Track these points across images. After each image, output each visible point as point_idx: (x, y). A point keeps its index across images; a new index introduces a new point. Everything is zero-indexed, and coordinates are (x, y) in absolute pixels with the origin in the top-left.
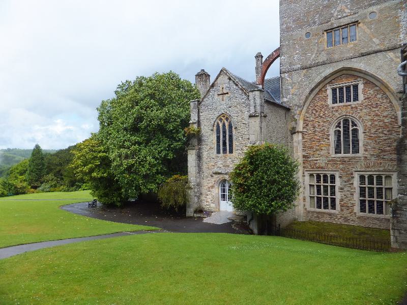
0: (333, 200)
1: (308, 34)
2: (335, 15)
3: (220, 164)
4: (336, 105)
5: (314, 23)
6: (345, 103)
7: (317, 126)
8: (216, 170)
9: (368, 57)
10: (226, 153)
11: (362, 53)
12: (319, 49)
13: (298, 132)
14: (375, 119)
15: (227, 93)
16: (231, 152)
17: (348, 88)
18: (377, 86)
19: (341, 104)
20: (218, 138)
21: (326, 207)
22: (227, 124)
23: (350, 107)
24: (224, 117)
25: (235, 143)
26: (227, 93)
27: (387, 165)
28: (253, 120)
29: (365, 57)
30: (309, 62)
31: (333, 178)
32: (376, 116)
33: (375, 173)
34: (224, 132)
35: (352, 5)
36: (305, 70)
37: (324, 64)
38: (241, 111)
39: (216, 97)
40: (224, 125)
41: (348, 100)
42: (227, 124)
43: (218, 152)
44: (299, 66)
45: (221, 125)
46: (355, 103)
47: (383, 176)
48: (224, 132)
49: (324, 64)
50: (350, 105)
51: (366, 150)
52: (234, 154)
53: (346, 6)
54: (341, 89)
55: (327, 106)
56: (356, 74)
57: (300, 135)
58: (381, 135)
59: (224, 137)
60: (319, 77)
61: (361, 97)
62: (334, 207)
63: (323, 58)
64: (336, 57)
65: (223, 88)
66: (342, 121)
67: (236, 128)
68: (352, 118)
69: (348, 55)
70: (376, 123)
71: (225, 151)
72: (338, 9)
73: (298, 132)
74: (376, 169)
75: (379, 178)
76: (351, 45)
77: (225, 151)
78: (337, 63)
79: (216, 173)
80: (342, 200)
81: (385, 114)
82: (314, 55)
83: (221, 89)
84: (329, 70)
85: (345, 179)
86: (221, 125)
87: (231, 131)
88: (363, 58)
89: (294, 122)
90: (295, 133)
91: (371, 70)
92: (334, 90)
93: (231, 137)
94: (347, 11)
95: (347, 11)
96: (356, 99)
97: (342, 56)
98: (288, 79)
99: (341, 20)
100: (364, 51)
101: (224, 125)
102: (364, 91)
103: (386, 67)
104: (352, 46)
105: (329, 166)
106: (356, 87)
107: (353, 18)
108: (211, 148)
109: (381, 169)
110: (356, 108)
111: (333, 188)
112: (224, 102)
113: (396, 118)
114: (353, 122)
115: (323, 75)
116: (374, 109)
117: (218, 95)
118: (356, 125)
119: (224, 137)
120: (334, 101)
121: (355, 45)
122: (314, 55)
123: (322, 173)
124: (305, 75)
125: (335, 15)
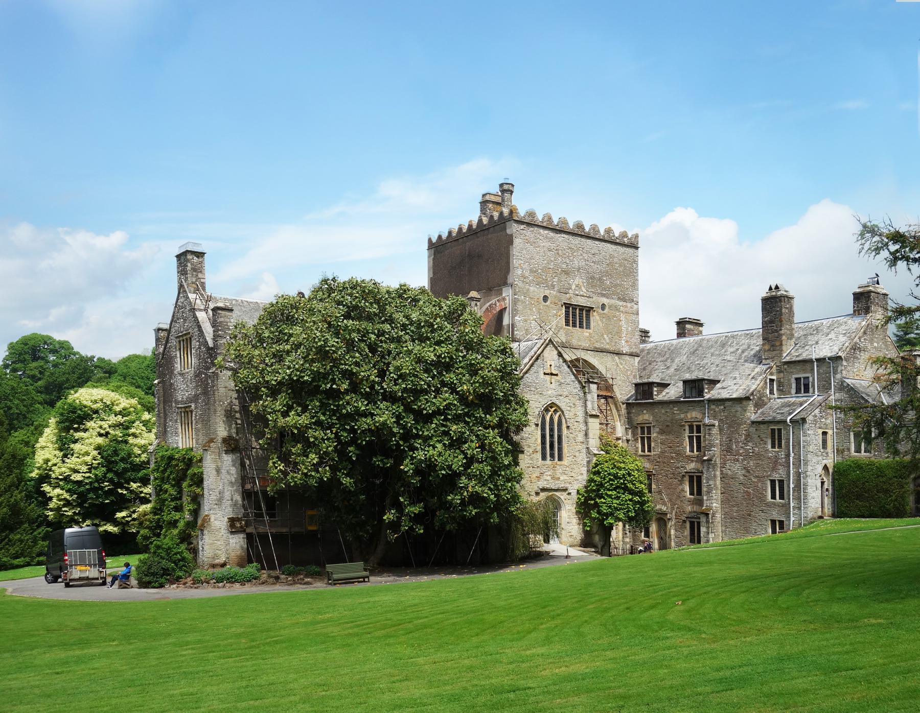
1: (545, 298)
5: (553, 286)
8: (542, 484)
15: (557, 375)
16: (560, 459)
20: (543, 437)
24: (552, 407)
25: (565, 445)
28: (591, 420)
34: (552, 430)
35: (588, 283)
40: (552, 419)
43: (544, 458)
45: (548, 418)
48: (552, 430)
52: (565, 462)
59: (552, 436)
64: (575, 342)
67: (568, 427)
71: (552, 456)
76: (586, 333)
77: (552, 456)
79: (543, 490)
86: (548, 418)
87: (560, 430)
91: (601, 369)
93: (560, 437)
100: (598, 345)
101: (552, 419)
108: (535, 451)
112: (553, 386)
119: (552, 436)
121: (591, 336)
125: (573, 287)
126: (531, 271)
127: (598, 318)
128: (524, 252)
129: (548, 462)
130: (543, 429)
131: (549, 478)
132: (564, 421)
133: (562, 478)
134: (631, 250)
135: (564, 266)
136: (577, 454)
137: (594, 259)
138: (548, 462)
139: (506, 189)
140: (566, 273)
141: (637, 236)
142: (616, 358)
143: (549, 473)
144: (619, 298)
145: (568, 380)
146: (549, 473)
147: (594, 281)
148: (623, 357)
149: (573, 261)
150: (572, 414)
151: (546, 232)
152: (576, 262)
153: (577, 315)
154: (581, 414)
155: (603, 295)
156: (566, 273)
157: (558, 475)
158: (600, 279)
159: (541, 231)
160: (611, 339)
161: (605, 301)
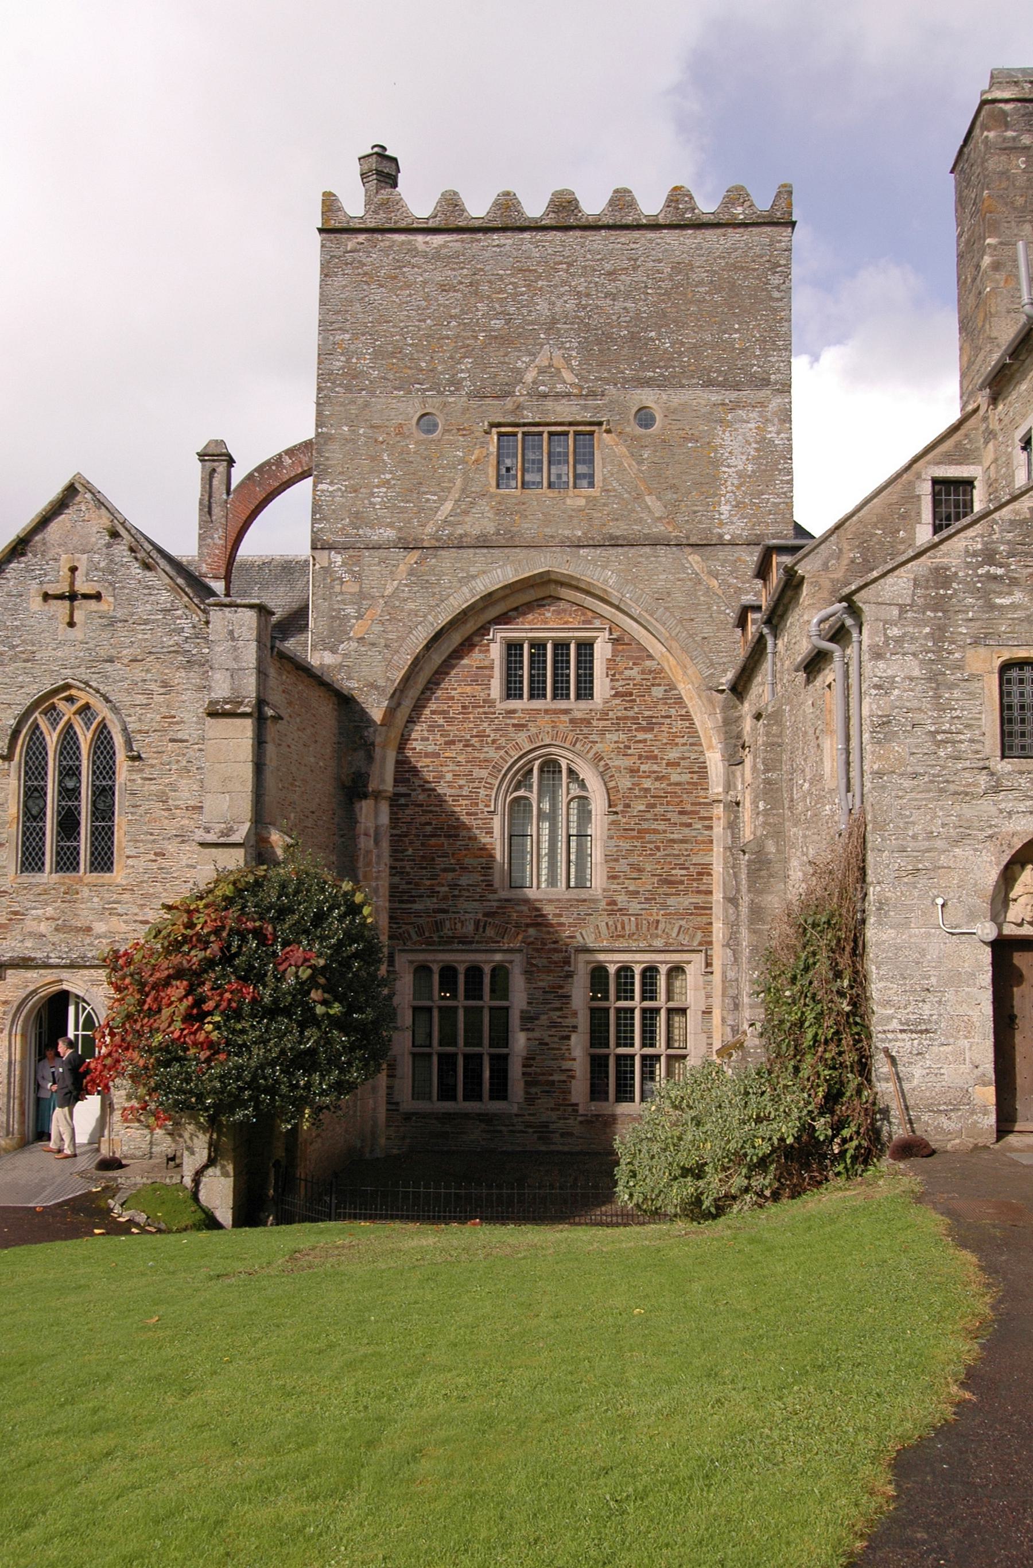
0: (500, 1064)
2: (529, 377)
3: (40, 920)
4: (514, 704)
6: (547, 703)
7: (449, 777)
9: (632, 552)
10: (76, 869)
11: (612, 537)
12: (463, 489)
13: (377, 795)
14: (643, 768)
15: (98, 597)
16: (102, 860)
17: (561, 646)
18: (650, 657)
19: (537, 704)
21: (473, 1093)
22: (85, 739)
23: (565, 718)
26: (98, 597)
27: (676, 930)
29: (620, 550)
30: (430, 529)
31: (500, 973)
32: (648, 758)
33: (638, 957)
34: (69, 772)
36: (414, 556)
37: (483, 543)
38: (165, 684)
39: (36, 603)
41: (560, 692)
42: (85, 739)
43: (31, 859)
44: (390, 534)
46: (583, 704)
47: (663, 969)
48: (69, 772)
49: (483, 543)
50: (566, 712)
51: (612, 877)
52: (119, 875)
53: (567, 359)
54: (539, 646)
55: (491, 703)
56: (589, 601)
57: (385, 808)
58: (661, 826)
59: (69, 794)
60: (465, 589)
61: (601, 686)
62: (500, 1091)
63: (481, 521)
64: (529, 528)
65: (73, 570)
66: (537, 763)
68: (570, 756)
69: (567, 533)
70: (647, 784)
72: (542, 360)
73: (377, 795)
74: (643, 945)
75: (650, 973)
76: (576, 499)
77: (67, 862)
78: (533, 552)
80: (528, 1061)
81: (673, 754)
82: (448, 506)
83: (65, 572)
84: (499, 573)
85: (545, 981)
86: (52, 740)
88: (612, 551)
89: (361, 754)
90: (365, 796)
92: (513, 648)
93: (104, 794)
94: (568, 376)
95: (568, 376)
96: (585, 691)
97: (548, 531)
98: (347, 577)
99: (549, 404)
100: (618, 529)
102: (613, 670)
103: (679, 597)
104: (582, 502)
105: (490, 932)
106: (586, 648)
107: (585, 408)
109: (659, 943)
110: (588, 722)
111: (501, 1016)
112: (76, 633)
113: (702, 771)
114: (571, 772)
115: (484, 585)
116: (641, 736)
117: (46, 597)
118: (582, 785)
119: (69, 794)
120: (512, 691)
122: (448, 506)
123: (461, 960)
124: (411, 573)
125: (529, 377)
126: (378, 354)
127: (622, 450)
128: (357, 307)
129: (48, 877)
130: (34, 770)
131: (43, 928)
132: (118, 740)
133: (100, 927)
134: (760, 236)
135: (497, 323)
136: (171, 847)
137: (611, 288)
138: (48, 877)
139: (382, 170)
140: (503, 340)
141: (786, 192)
142: (694, 560)
143: (50, 911)
144: (709, 384)
145: (142, 610)
146: (50, 911)
147: (598, 344)
148: (722, 553)
149: (531, 302)
150: (153, 717)
151: (438, 239)
152: (542, 306)
153: (542, 446)
154: (190, 708)
155: (647, 383)
156: (503, 340)
157: (85, 915)
158: (633, 337)
159: (420, 238)
160: (673, 510)
161: (647, 397)
